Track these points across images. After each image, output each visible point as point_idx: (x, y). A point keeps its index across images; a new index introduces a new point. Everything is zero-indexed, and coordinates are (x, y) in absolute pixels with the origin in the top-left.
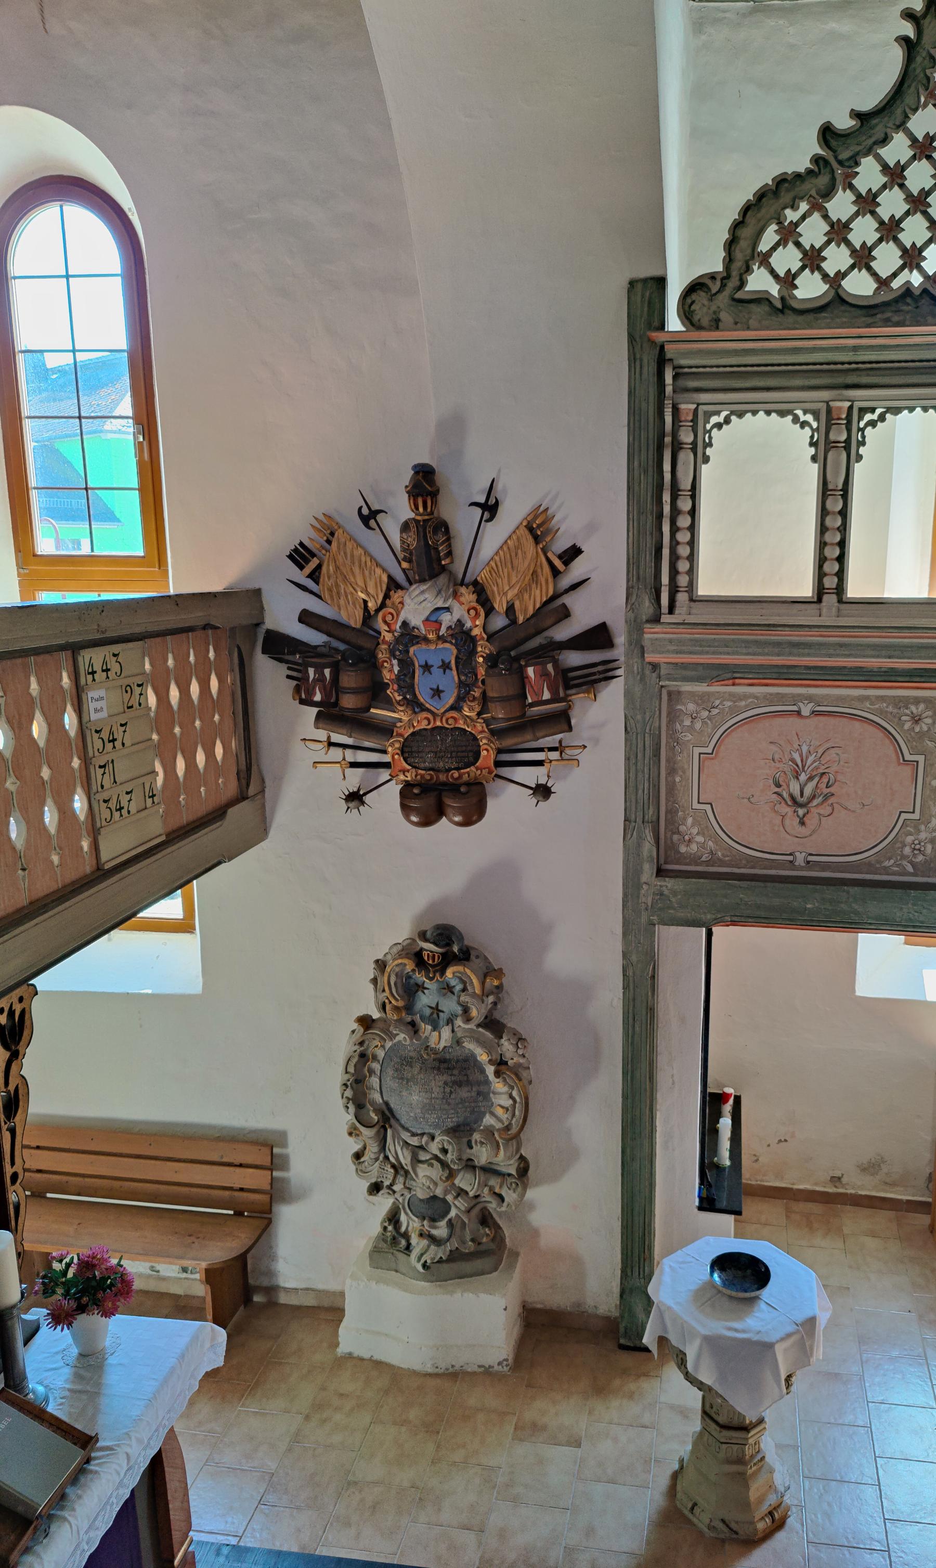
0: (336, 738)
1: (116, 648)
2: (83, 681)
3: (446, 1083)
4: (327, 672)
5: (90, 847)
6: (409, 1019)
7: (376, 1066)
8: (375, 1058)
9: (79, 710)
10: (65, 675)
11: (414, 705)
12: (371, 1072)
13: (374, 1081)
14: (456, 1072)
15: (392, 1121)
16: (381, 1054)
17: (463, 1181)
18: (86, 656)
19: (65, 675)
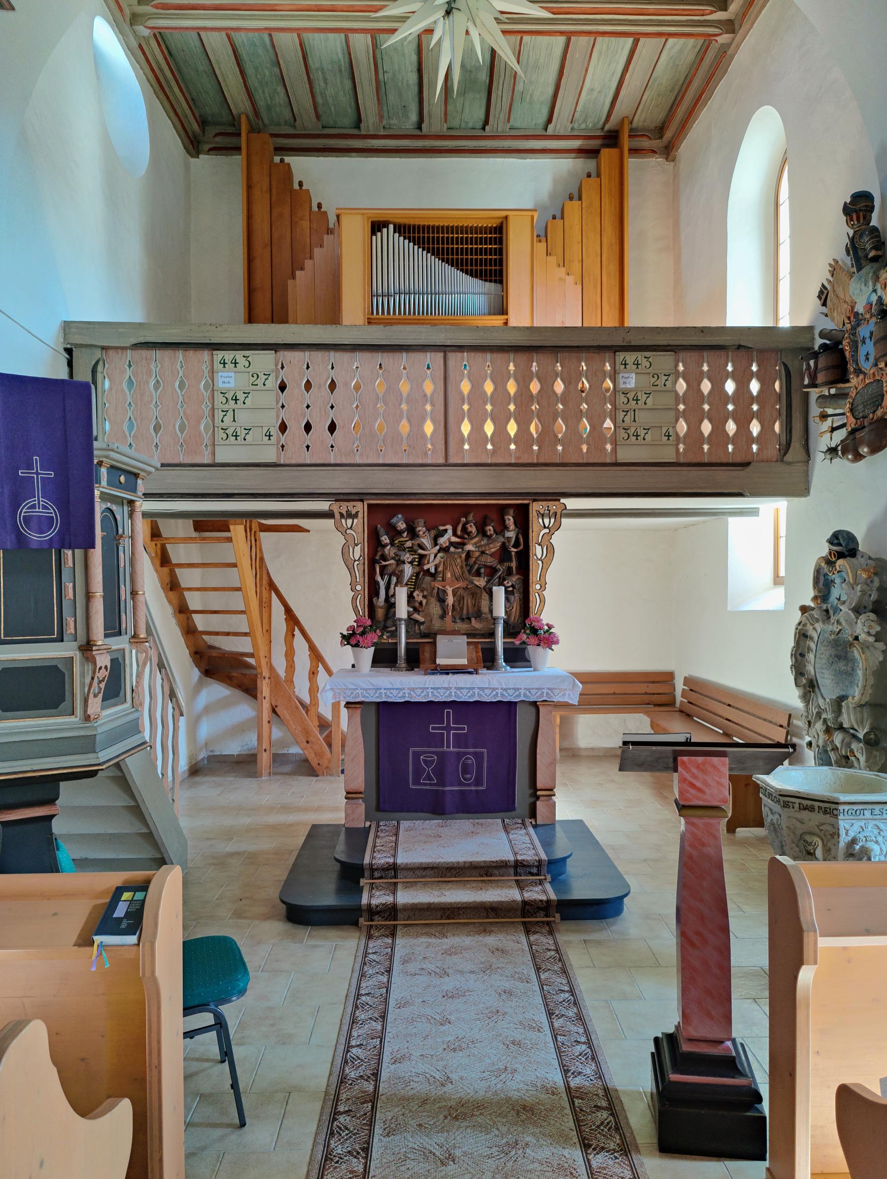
0: (830, 411)
1: (648, 354)
2: (617, 368)
3: (831, 655)
4: (812, 363)
5: (612, 449)
6: (824, 607)
7: (813, 646)
8: (812, 638)
9: (614, 382)
10: (607, 364)
11: (859, 371)
12: (809, 649)
13: (811, 656)
14: (839, 648)
15: (817, 689)
16: (815, 636)
17: (838, 738)
18: (621, 356)
19: (607, 364)
